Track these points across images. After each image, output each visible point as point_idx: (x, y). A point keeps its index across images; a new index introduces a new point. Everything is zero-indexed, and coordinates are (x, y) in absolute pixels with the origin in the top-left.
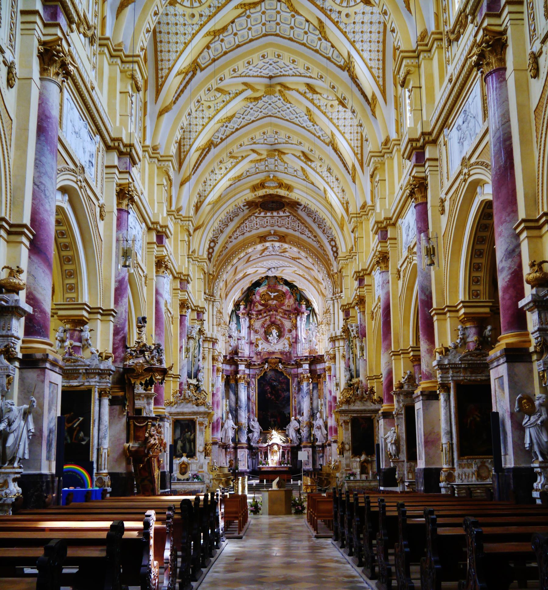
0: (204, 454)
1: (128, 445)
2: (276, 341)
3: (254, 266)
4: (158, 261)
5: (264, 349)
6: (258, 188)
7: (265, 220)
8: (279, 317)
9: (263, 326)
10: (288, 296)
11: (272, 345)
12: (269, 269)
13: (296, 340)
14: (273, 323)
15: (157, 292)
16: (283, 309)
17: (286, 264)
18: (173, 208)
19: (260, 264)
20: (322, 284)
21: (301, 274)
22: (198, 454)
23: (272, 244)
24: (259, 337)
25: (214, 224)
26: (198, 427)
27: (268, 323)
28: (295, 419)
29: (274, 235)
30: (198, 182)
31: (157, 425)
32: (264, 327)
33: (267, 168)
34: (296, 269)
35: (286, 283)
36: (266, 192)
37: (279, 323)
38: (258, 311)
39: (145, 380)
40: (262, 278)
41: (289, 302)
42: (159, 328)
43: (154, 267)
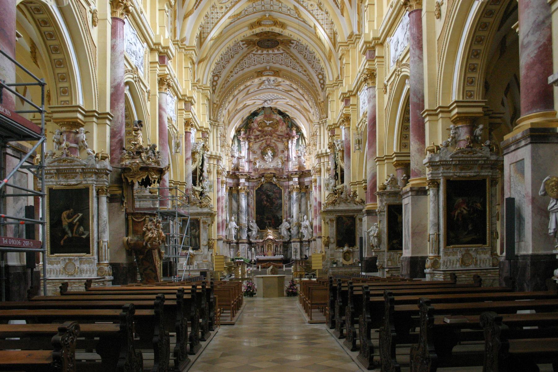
0: (207, 247)
1: (126, 239)
2: (271, 160)
3: (253, 98)
4: (161, 79)
5: (261, 166)
6: (255, 26)
7: (262, 57)
8: (273, 141)
9: (260, 148)
10: (281, 124)
11: (267, 163)
12: (265, 101)
13: (288, 159)
14: (268, 145)
15: (160, 107)
16: (276, 134)
17: (280, 96)
18: (178, 38)
19: (257, 97)
20: (310, 112)
21: (292, 104)
22: (202, 247)
23: (268, 78)
24: (256, 157)
25: (216, 57)
26: (201, 225)
27: (264, 145)
28: (286, 221)
29: (269, 70)
30: (199, 16)
31: (155, 220)
32: (261, 149)
33: (263, 7)
34: (288, 100)
35: (280, 113)
36: (262, 29)
37: (273, 145)
38: (256, 136)
39: (142, 179)
40: (259, 109)
41: (282, 129)
42: (163, 139)
43: (157, 84)
